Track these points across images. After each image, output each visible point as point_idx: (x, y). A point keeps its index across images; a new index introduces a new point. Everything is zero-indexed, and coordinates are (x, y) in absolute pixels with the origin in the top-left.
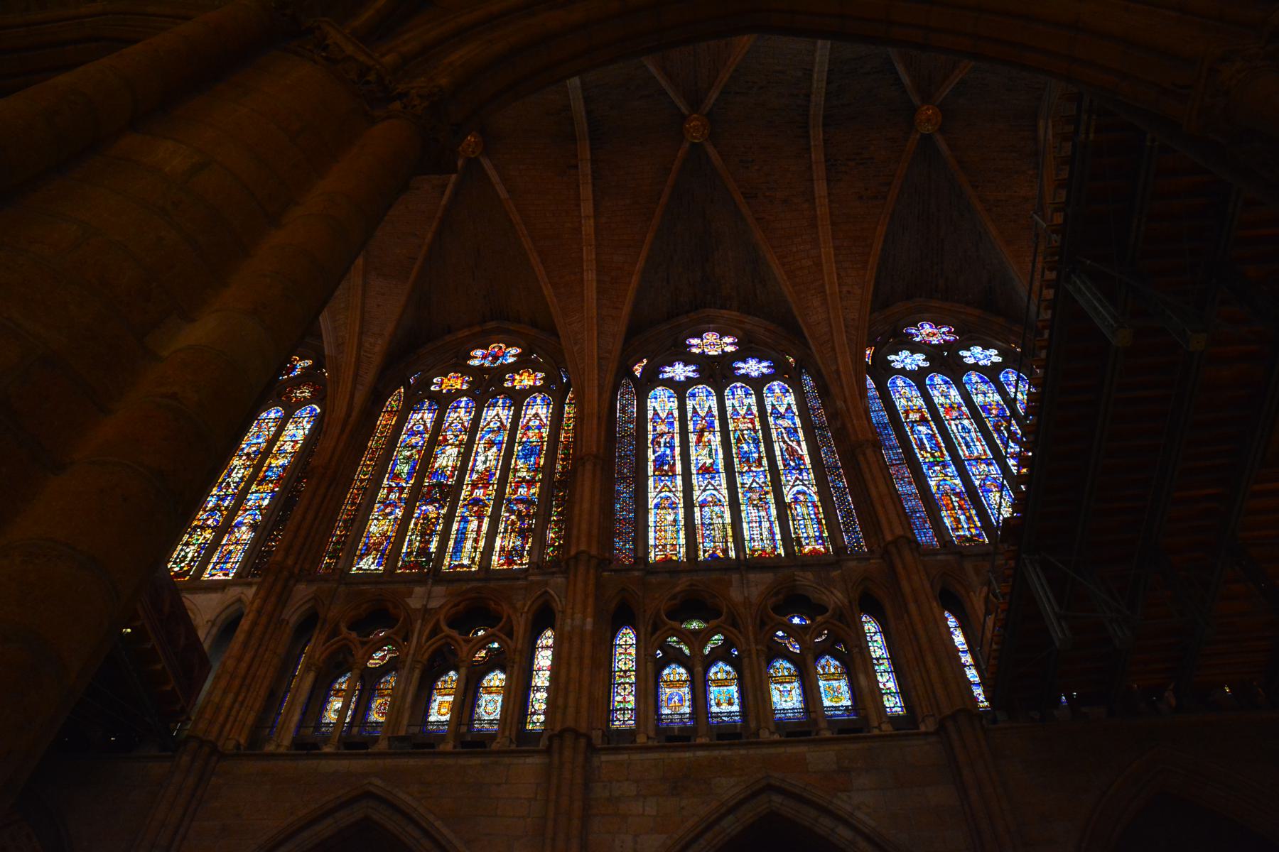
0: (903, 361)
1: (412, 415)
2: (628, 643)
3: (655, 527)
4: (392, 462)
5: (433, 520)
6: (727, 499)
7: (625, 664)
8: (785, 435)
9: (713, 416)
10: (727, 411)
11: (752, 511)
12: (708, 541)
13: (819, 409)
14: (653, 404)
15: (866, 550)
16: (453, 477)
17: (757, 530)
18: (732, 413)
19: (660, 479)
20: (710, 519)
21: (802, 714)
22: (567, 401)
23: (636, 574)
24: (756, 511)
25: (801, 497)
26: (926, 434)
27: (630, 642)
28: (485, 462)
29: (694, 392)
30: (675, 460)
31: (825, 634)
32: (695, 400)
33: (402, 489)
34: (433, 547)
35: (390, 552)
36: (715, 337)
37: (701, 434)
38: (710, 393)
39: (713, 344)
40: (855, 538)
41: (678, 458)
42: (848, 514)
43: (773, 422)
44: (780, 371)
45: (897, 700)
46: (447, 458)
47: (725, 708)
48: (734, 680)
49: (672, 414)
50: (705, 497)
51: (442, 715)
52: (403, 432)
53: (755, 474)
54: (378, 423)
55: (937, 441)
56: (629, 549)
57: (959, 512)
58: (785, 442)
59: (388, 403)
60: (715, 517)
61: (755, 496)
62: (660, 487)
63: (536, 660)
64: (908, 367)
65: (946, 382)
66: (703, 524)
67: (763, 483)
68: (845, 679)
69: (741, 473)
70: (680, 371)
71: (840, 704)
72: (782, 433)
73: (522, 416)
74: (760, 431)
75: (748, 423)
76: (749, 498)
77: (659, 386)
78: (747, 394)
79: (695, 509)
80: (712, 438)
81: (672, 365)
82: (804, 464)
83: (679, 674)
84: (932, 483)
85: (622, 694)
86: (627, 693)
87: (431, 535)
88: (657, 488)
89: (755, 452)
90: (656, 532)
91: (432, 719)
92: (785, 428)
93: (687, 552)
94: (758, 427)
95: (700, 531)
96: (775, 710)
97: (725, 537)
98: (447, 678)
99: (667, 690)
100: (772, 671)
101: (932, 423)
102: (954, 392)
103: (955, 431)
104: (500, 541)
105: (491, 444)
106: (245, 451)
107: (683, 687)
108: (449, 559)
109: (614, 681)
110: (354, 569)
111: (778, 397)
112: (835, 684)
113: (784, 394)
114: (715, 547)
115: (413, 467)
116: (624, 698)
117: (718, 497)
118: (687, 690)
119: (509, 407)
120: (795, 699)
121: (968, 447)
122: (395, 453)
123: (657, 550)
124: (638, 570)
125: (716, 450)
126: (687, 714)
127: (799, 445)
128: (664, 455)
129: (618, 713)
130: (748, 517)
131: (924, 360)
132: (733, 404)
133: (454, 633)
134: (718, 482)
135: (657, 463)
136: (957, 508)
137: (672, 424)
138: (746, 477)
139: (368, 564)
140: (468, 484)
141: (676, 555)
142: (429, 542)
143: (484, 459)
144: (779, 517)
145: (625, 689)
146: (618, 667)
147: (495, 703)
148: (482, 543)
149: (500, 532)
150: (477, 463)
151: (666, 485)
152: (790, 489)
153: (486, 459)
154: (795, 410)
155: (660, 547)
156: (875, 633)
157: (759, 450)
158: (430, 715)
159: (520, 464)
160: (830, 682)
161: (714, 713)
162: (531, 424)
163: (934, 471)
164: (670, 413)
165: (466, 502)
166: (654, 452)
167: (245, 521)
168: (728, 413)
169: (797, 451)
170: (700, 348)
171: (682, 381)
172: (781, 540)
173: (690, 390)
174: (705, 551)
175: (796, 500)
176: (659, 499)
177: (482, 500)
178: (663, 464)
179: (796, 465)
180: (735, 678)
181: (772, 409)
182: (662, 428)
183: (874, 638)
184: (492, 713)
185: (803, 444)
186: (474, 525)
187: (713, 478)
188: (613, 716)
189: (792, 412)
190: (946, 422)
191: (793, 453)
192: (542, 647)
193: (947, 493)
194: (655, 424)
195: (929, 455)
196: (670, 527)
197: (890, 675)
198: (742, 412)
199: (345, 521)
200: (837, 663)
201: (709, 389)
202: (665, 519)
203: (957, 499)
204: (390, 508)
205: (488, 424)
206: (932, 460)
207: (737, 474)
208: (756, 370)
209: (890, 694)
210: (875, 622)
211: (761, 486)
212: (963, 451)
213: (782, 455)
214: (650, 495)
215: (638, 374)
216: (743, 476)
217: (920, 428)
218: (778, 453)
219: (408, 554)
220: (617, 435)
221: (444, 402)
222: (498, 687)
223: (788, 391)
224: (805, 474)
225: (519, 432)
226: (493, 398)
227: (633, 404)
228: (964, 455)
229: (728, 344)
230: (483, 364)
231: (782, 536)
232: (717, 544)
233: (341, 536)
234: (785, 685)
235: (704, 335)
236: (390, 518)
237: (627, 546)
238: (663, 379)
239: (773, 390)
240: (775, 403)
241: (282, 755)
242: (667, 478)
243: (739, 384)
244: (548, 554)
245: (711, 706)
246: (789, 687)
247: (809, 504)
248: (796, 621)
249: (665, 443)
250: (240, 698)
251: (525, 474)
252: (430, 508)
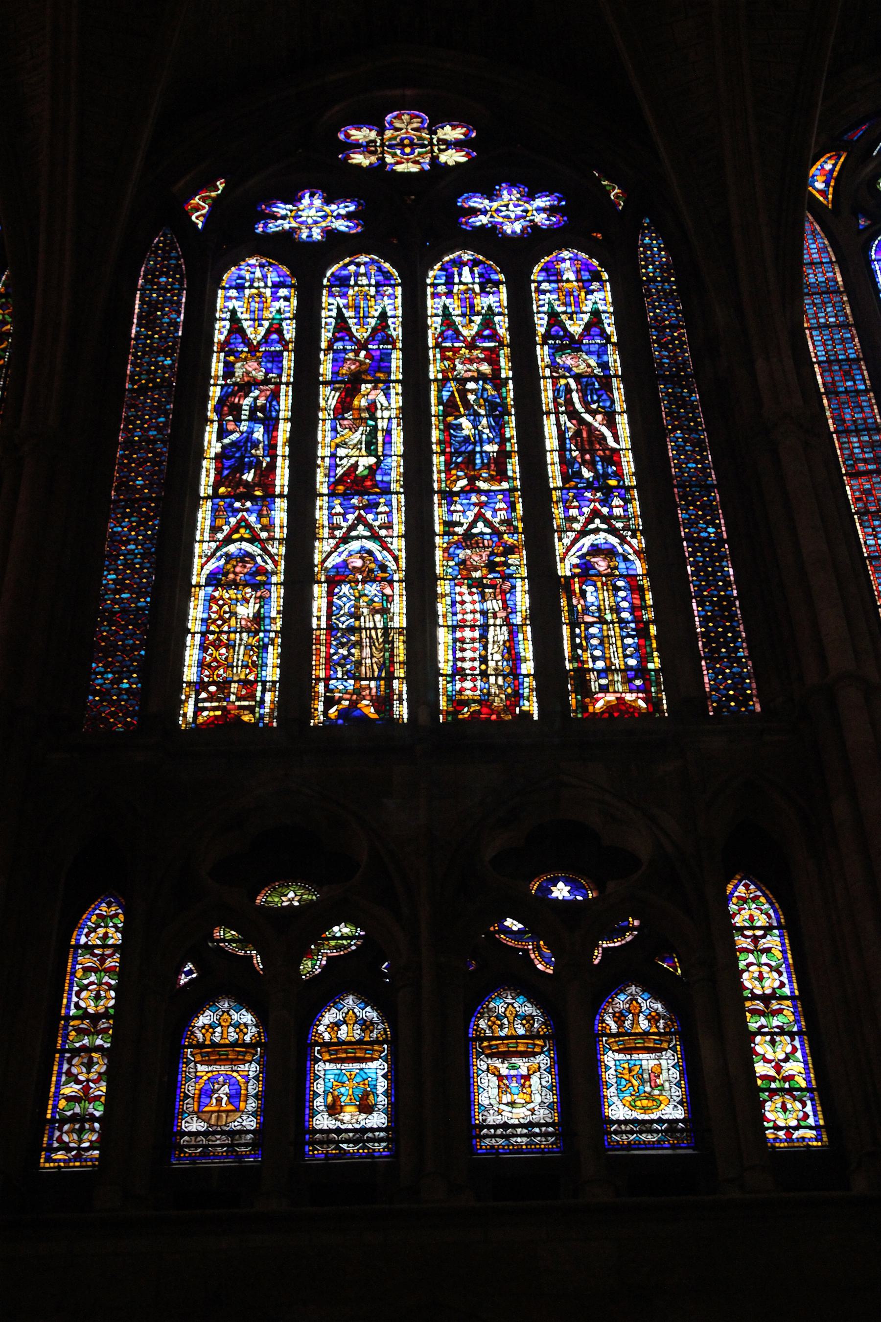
2: (111, 942)
3: (203, 634)
6: (403, 563)
7: (98, 997)
8: (575, 396)
9: (389, 340)
10: (427, 327)
11: (467, 598)
12: (340, 675)
13: (674, 327)
14: (230, 305)
15: (758, 708)
17: (474, 650)
18: (441, 334)
19: (231, 505)
20: (351, 615)
21: (552, 1139)
24: (476, 597)
25: (601, 564)
29: (345, 272)
30: (274, 457)
31: (634, 928)
32: (344, 295)
38: (387, 276)
40: (732, 676)
41: (282, 450)
43: (547, 359)
45: (809, 1109)
47: (350, 1118)
48: (381, 1043)
49: (280, 332)
50: (344, 556)
53: (484, 498)
58: (573, 414)
60: (366, 611)
61: (478, 558)
62: (226, 528)
66: (331, 629)
67: (502, 522)
68: (674, 1049)
69: (449, 496)
71: (654, 1116)
72: (568, 390)
75: (480, 361)
76: (463, 562)
77: (251, 256)
78: (487, 284)
79: (316, 587)
80: (382, 399)
82: (619, 475)
83: (237, 1026)
85: (81, 1078)
86: (93, 1076)
88: (220, 529)
89: (490, 441)
90: (203, 648)
92: (577, 377)
93: (281, 705)
94: (506, 373)
95: (323, 649)
96: (481, 1127)
97: (387, 665)
100: (483, 1024)
107: (244, 1062)
109: (64, 1042)
111: (569, 293)
112: (648, 1061)
114: (358, 691)
116: (86, 1089)
117: (380, 558)
118: (253, 1069)
120: (537, 1099)
123: (203, 695)
125: (388, 432)
126: (248, 1132)
127: (612, 425)
128: (248, 441)
129: (66, 1127)
130: (454, 614)
132: (445, 307)
134: (382, 518)
135: (228, 463)
137: (276, 358)
138: (459, 507)
144: (536, 615)
145: (89, 1065)
146: (77, 1006)
151: (243, 523)
152: (573, 543)
154: (610, 330)
155: (213, 689)
156: (768, 929)
157: (502, 435)
160: (635, 1056)
161: (322, 1131)
164: (276, 329)
166: (222, 433)
168: (430, 332)
170: (374, 153)
171: (318, 243)
172: (535, 676)
173: (334, 268)
174: (329, 702)
175: (585, 571)
176: (223, 561)
179: (597, 476)
180: (385, 1041)
181: (550, 325)
183: (764, 943)
185: (622, 422)
187: (371, 507)
188: (51, 1138)
189: (603, 334)
191: (591, 443)
194: (232, 358)
196: (245, 635)
197: (797, 1043)
200: (658, 1006)
201: (387, 265)
202: (235, 614)
207: (436, 498)
208: (518, 218)
209: (790, 1091)
210: (769, 901)
211: (496, 532)
213: (562, 449)
215: (198, 220)
216: (450, 503)
218: (551, 443)
220: (128, 386)
223: (597, 277)
224: (616, 502)
227: (179, 303)
232: (363, 683)
235: (388, 118)
238: (267, 237)
239: (560, 273)
242: (248, 504)
245: (314, 1113)
246: (523, 1066)
248: (561, 891)
249: (253, 409)
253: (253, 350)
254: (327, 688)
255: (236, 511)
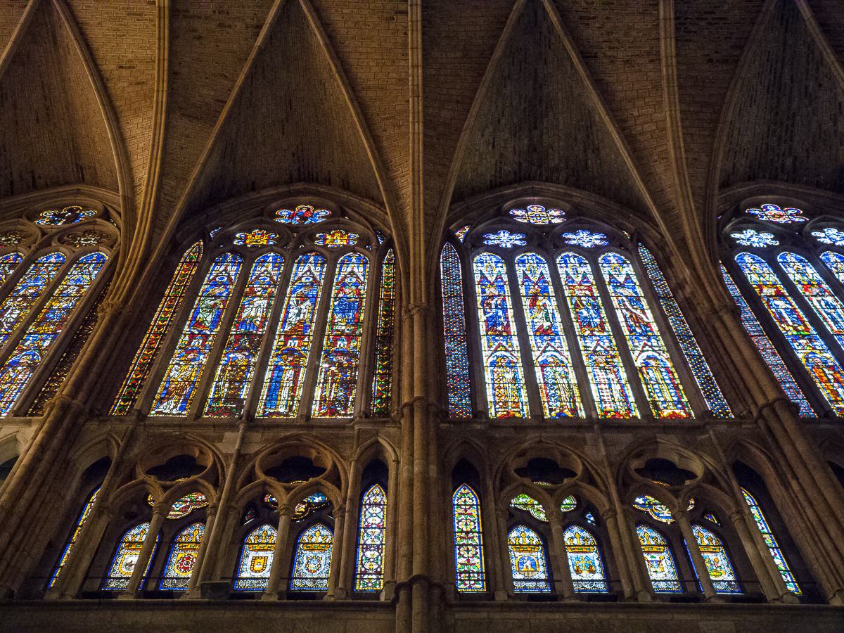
0: (749, 240)
1: (214, 267)
3: (493, 384)
4: (193, 310)
5: (243, 368)
6: (570, 360)
7: (466, 524)
8: (627, 303)
9: (545, 282)
11: (600, 373)
13: (661, 280)
14: (479, 268)
15: (733, 417)
16: (263, 327)
22: (385, 261)
23: (478, 427)
25: (653, 363)
26: (785, 309)
27: (470, 502)
28: (298, 315)
30: (508, 322)
33: (206, 337)
34: (244, 394)
35: (197, 395)
36: (540, 209)
37: (535, 297)
39: (536, 214)
40: (719, 405)
41: (511, 319)
42: (707, 380)
43: (612, 291)
44: (615, 242)
46: (256, 309)
47: (585, 575)
49: (501, 278)
51: (256, 572)
52: (205, 282)
53: (598, 338)
54: (176, 272)
55: (798, 315)
56: (466, 404)
57: (836, 385)
58: (627, 310)
59: (186, 254)
60: (559, 377)
61: (601, 359)
62: (494, 347)
63: (363, 517)
64: (755, 245)
65: (801, 261)
66: (546, 384)
68: (722, 552)
70: (505, 239)
71: (721, 578)
73: (337, 273)
74: (599, 298)
80: (548, 303)
81: (495, 232)
82: (651, 331)
84: (800, 356)
85: (466, 556)
87: (241, 382)
91: (244, 575)
92: (626, 297)
93: (531, 410)
94: (596, 294)
98: (261, 532)
99: (517, 554)
101: (790, 298)
102: (810, 270)
103: (818, 306)
104: (320, 391)
105: (303, 298)
106: (21, 293)
108: (262, 407)
110: (153, 412)
111: (615, 268)
113: (621, 265)
115: (219, 316)
116: (468, 560)
118: (539, 555)
119: (322, 264)
120: (666, 570)
121: (836, 323)
122: (196, 302)
123: (497, 406)
124: (481, 423)
125: (553, 314)
127: (644, 313)
131: (772, 239)
133: (270, 480)
134: (558, 344)
136: (832, 381)
137: (502, 287)
139: (169, 408)
140: (280, 335)
141: (519, 412)
142: (239, 389)
143: (296, 311)
145: (468, 551)
147: (319, 561)
148: (299, 392)
149: (320, 383)
150: (290, 315)
152: (640, 354)
153: (298, 311)
155: (501, 404)
158: (242, 572)
159: (338, 318)
162: (347, 281)
163: (800, 344)
165: (280, 352)
166: (485, 313)
167: (21, 361)
169: (642, 318)
173: (518, 257)
174: (551, 410)
175: (647, 365)
177: (296, 351)
178: (495, 325)
179: (643, 331)
181: (610, 279)
182: (491, 291)
184: (315, 571)
185: (648, 312)
186: (290, 373)
187: (552, 340)
189: (632, 282)
190: (806, 298)
192: (370, 504)
193: (818, 366)
195: (791, 328)
197: (776, 551)
198: (578, 280)
199: (142, 365)
200: (711, 535)
201: (539, 257)
203: (832, 372)
204: (192, 354)
205: (300, 279)
206: (795, 333)
207: (578, 338)
211: (606, 350)
212: (831, 327)
213: (626, 321)
214: (484, 353)
216: (585, 340)
217: (776, 302)
218: (621, 319)
219: (216, 400)
221: (248, 256)
222: (321, 543)
223: (625, 262)
224: (653, 340)
225: (334, 288)
226: (303, 254)
228: (832, 330)
229: (555, 217)
230: (291, 223)
231: (636, 399)
233: (137, 380)
234: (653, 554)
236: (193, 363)
237: (464, 401)
240: (613, 273)
241: (69, 604)
242: (501, 338)
243: (571, 254)
244: (374, 405)
246: (657, 557)
247: (662, 370)
249: (496, 306)
250: (17, 540)
251: (343, 328)
252: (239, 356)
253: (492, 284)
254: (549, 405)
255: (497, 340)
